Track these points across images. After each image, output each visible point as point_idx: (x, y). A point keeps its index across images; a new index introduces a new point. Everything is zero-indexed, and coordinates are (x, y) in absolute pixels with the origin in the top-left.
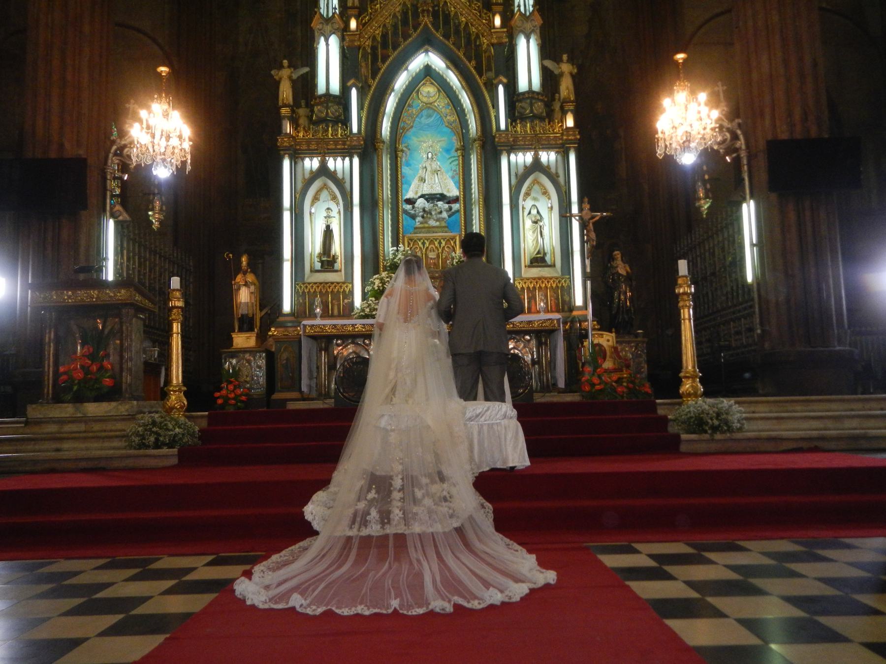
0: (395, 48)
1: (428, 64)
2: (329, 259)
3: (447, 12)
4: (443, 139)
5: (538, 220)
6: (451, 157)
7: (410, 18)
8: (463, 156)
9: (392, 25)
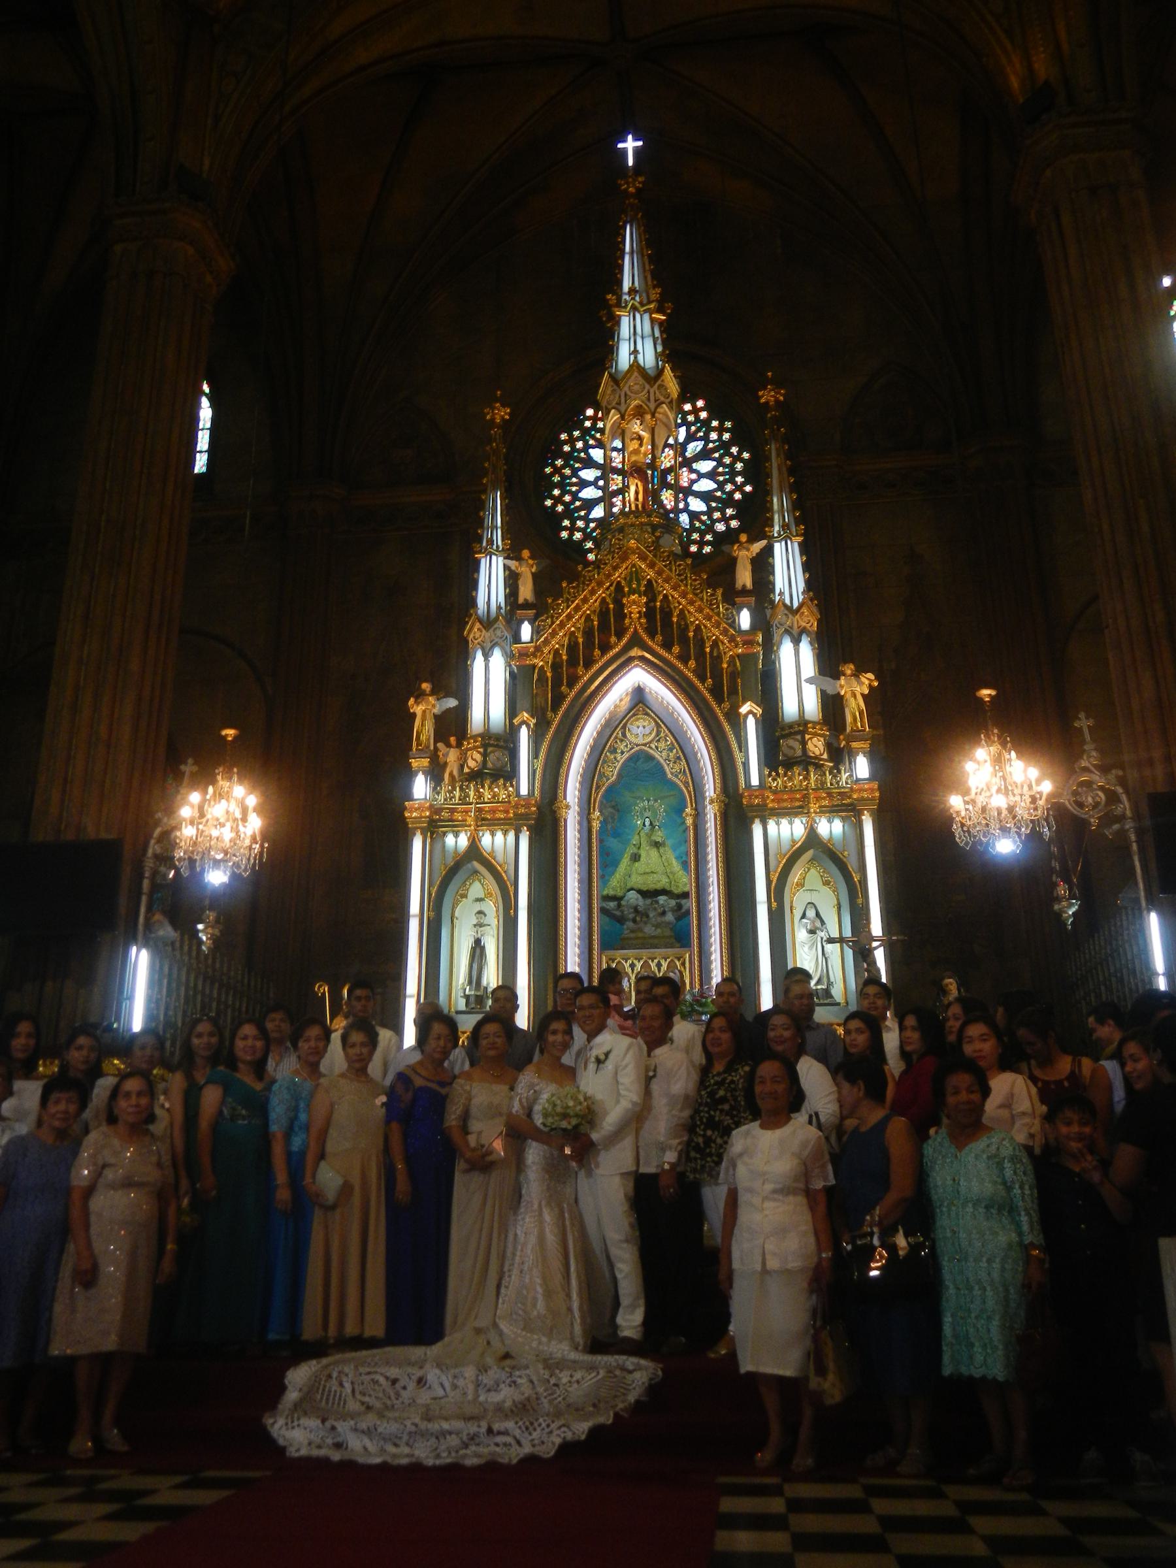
0: (587, 666)
1: (639, 686)
2: (478, 994)
3: (668, 610)
4: (672, 793)
5: (818, 929)
7: (612, 620)
9: (584, 633)
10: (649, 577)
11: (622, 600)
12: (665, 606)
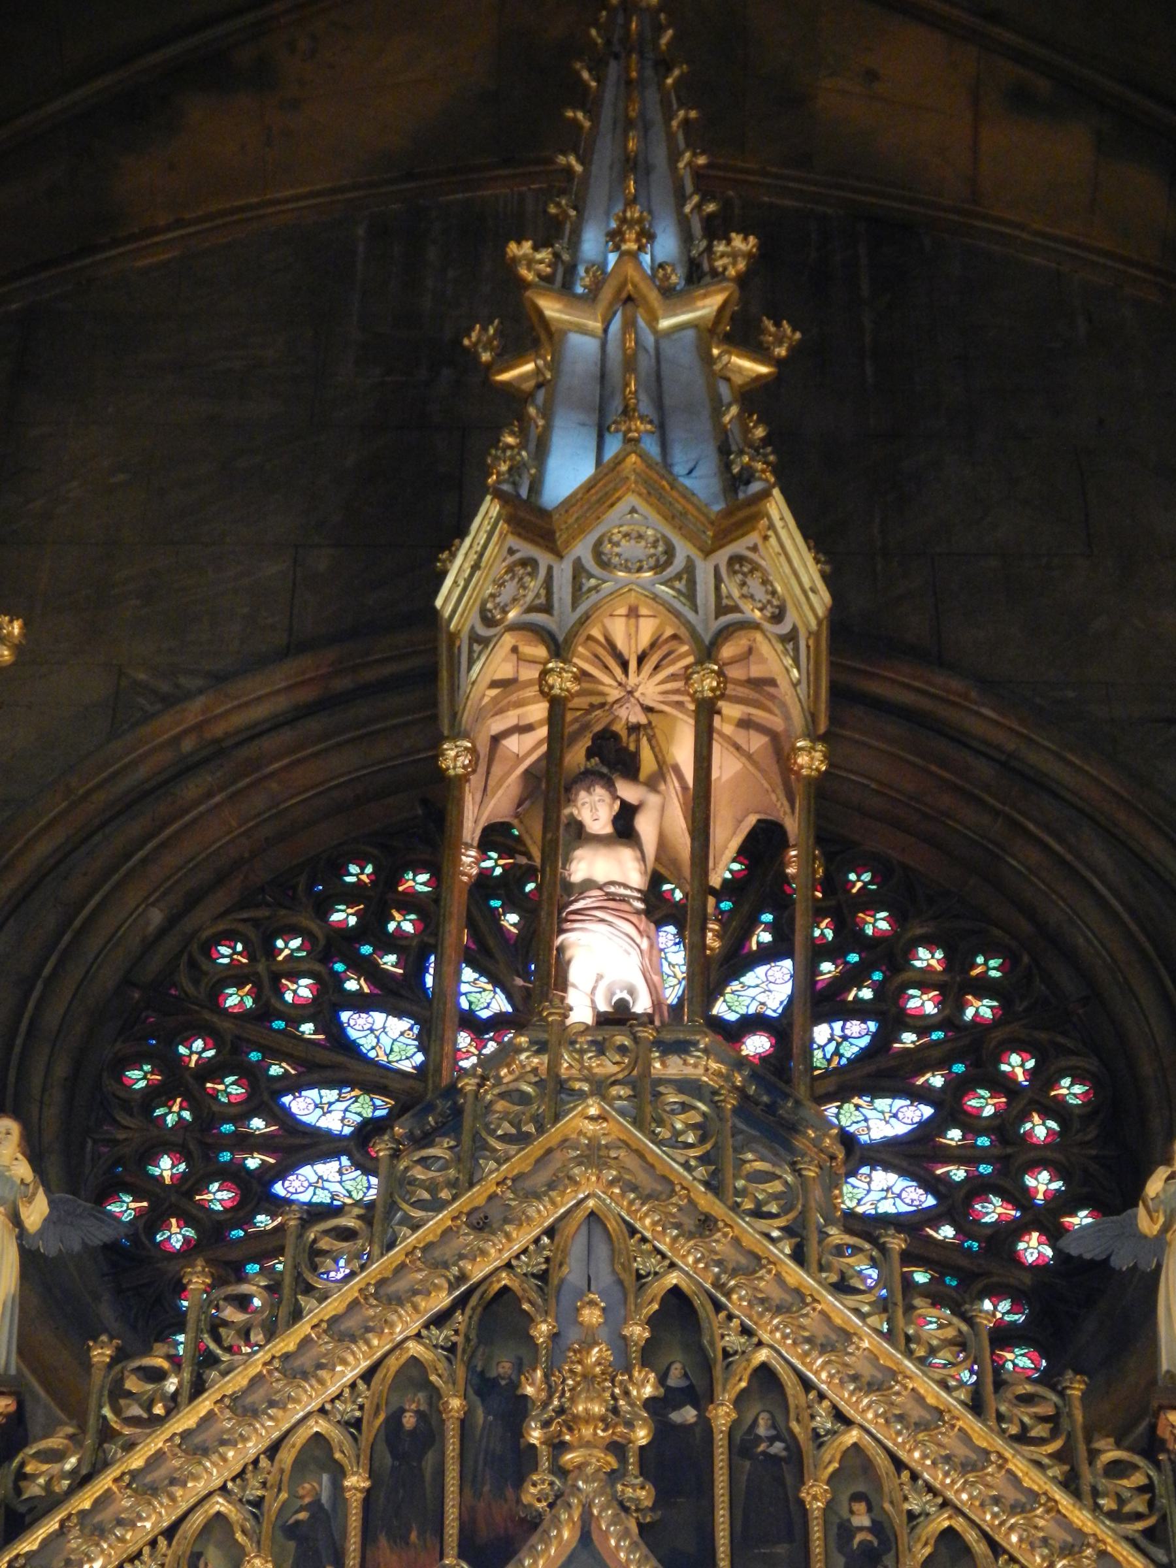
3: (778, 1448)
10: (673, 1279)
11: (515, 1385)
12: (762, 1430)
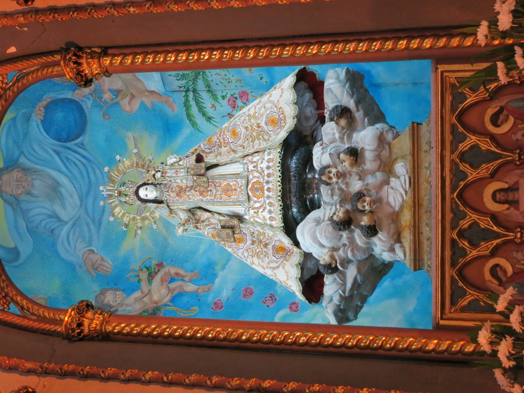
6: (189, 116)
8: (105, 51)
